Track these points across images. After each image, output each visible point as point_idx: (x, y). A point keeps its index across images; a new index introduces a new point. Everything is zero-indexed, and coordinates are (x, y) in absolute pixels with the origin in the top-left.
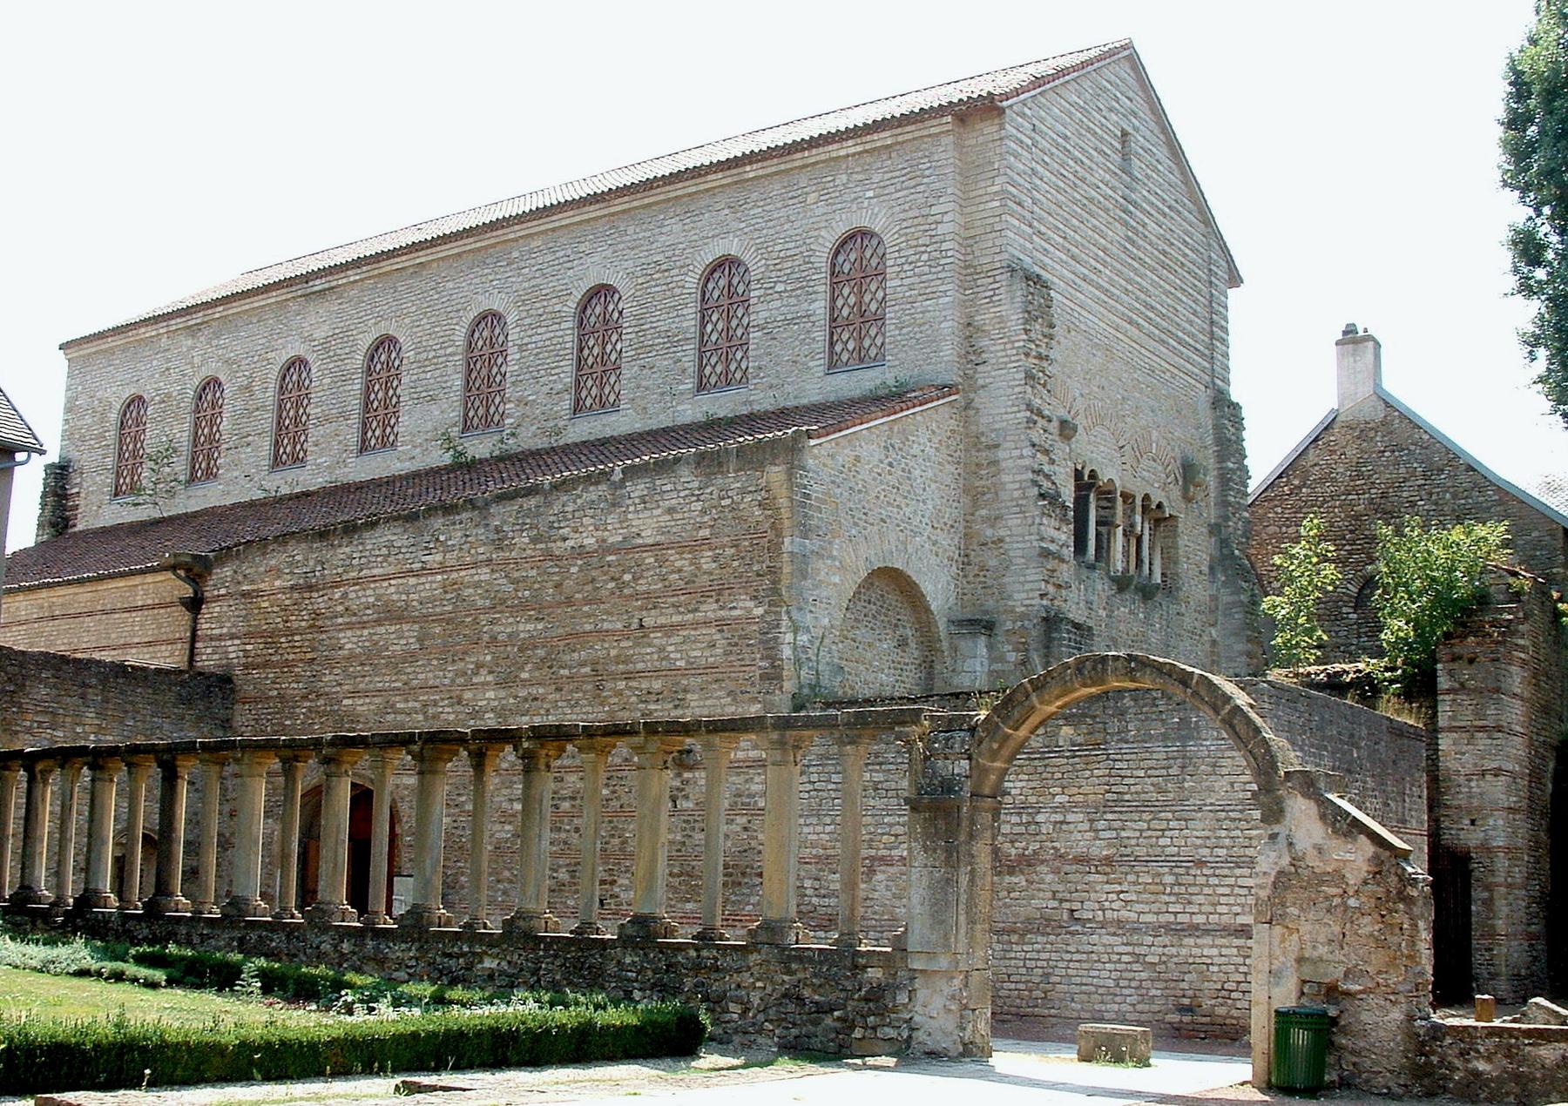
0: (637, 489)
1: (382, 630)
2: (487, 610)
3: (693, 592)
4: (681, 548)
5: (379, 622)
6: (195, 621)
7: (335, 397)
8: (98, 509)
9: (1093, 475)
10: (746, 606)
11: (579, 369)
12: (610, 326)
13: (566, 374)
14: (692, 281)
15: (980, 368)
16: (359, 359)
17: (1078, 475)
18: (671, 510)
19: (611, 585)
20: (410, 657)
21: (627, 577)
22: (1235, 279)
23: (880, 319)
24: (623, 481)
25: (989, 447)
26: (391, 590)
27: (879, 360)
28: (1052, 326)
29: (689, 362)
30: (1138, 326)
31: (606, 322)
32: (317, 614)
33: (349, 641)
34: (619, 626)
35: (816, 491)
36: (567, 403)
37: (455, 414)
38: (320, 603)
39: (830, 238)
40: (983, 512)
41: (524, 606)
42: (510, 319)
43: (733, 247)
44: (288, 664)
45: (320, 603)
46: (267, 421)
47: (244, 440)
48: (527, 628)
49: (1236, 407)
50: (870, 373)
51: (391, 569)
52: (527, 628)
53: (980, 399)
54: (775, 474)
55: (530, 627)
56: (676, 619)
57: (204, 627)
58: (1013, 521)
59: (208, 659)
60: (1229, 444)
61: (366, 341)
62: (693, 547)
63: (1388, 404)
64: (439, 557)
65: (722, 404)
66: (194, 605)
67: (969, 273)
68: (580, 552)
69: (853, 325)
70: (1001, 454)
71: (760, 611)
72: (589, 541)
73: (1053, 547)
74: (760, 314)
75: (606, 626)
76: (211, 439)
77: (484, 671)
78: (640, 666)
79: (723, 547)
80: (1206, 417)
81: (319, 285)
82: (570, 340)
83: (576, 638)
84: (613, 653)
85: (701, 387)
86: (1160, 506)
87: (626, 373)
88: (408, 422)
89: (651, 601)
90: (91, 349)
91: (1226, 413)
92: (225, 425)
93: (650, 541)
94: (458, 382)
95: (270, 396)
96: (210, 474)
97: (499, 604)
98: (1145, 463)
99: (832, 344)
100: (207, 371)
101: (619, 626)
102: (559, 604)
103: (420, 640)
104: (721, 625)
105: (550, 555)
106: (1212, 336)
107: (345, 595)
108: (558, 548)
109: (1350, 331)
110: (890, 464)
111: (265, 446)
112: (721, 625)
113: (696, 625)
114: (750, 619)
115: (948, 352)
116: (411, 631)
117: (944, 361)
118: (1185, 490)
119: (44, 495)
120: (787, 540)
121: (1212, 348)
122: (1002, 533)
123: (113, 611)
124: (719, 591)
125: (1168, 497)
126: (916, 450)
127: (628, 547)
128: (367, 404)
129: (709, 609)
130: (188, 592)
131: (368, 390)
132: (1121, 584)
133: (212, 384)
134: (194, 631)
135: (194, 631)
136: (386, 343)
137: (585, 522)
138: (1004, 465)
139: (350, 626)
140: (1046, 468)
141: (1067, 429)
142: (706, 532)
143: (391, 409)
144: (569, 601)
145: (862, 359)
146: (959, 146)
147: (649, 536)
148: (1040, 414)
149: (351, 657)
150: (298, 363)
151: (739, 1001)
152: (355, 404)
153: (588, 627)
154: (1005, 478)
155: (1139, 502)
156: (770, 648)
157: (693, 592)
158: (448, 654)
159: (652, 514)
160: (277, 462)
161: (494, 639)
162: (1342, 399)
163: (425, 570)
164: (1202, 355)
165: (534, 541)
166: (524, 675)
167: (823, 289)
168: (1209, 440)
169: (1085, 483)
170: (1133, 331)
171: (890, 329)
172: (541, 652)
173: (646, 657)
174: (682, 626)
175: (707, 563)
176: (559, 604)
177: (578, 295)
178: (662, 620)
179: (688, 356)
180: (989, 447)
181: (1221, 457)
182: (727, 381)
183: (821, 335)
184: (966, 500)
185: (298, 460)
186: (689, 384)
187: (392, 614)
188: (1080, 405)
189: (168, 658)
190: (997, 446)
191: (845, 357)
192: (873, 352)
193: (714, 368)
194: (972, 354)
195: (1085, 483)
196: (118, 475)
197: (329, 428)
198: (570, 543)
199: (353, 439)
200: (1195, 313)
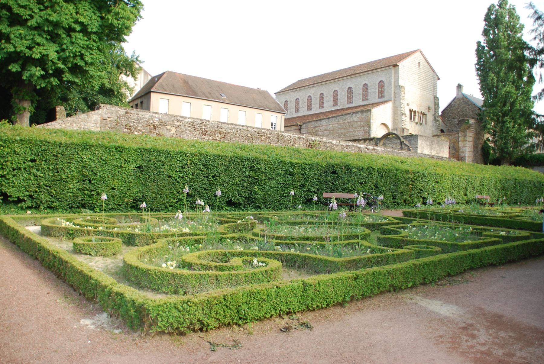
0: (354, 115)
3: (361, 127)
7: (316, 101)
10: (366, 128)
13: (346, 98)
16: (318, 96)
22: (439, 79)
26: (326, 127)
38: (317, 129)
43: (366, 82)
47: (303, 107)
48: (342, 131)
52: (342, 131)
60: (436, 105)
61: (319, 94)
63: (463, 95)
65: (366, 103)
68: (348, 122)
74: (370, 91)
83: (348, 132)
88: (325, 105)
89: (356, 128)
91: (436, 98)
94: (332, 99)
97: (339, 128)
109: (459, 84)
116: (328, 132)
124: (363, 127)
125: (426, 112)
127: (353, 122)
129: (362, 129)
132: (417, 123)
133: (297, 99)
136: (322, 94)
137: (348, 119)
141: (408, 105)
145: (382, 97)
150: (310, 96)
157: (361, 127)
162: (457, 94)
167: (377, 88)
173: (355, 134)
175: (362, 123)
182: (366, 100)
185: (311, 110)
187: (326, 130)
195: (411, 111)
199: (318, 107)
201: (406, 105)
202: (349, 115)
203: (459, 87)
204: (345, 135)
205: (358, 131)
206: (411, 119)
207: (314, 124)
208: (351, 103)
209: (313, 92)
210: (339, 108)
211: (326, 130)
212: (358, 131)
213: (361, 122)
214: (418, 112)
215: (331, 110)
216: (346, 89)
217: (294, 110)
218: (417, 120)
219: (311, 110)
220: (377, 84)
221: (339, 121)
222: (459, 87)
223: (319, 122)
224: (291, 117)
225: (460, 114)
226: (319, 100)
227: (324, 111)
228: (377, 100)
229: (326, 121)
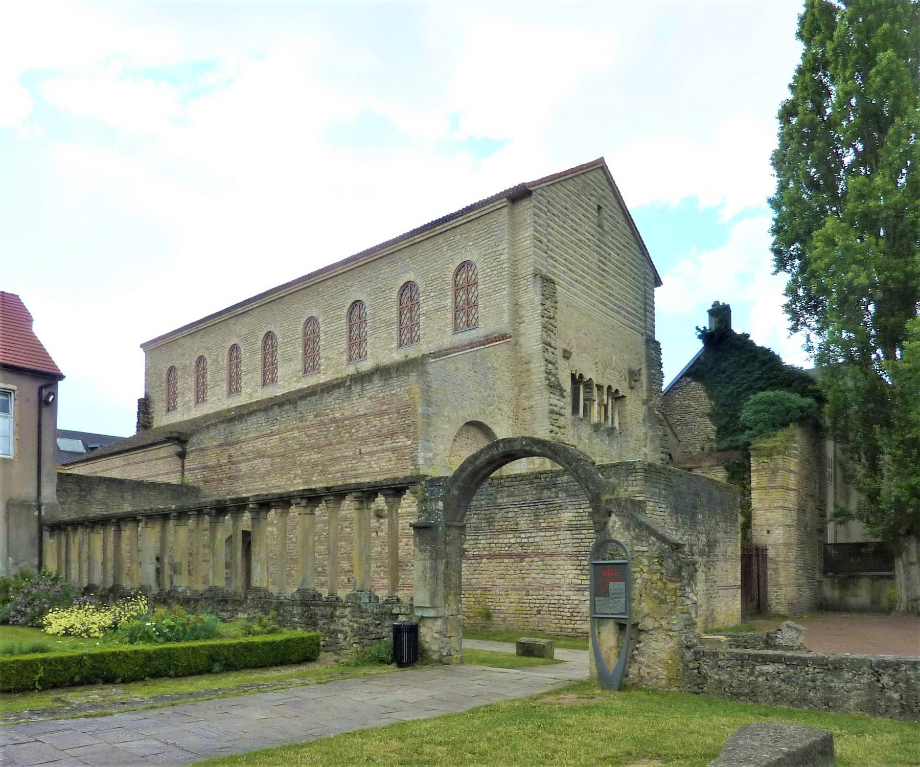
0: (356, 389)
1: (256, 462)
2: (297, 450)
3: (381, 436)
4: (375, 415)
5: (255, 458)
6: (183, 462)
8: (162, 420)
9: (581, 375)
11: (350, 340)
12: (362, 320)
13: (344, 344)
14: (395, 295)
15: (522, 325)
17: (573, 376)
18: (370, 398)
19: (347, 435)
20: (268, 473)
21: (354, 431)
23: (476, 305)
24: (350, 386)
25: (526, 363)
27: (476, 326)
28: (556, 302)
29: (395, 335)
30: (605, 305)
31: (360, 318)
32: (230, 456)
33: (244, 467)
34: (351, 453)
35: (435, 385)
36: (345, 357)
37: (300, 366)
40: (524, 394)
41: (312, 448)
42: (320, 320)
44: (221, 480)
46: (224, 374)
47: (216, 384)
48: (315, 457)
49: (658, 344)
50: (472, 332)
51: (258, 434)
52: (315, 457)
53: (522, 340)
54: (413, 377)
55: (315, 456)
56: (375, 449)
57: (188, 464)
58: (538, 397)
59: (189, 479)
64: (277, 427)
66: (182, 455)
68: (335, 420)
70: (532, 366)
71: (409, 443)
72: (338, 415)
73: (556, 409)
75: (346, 454)
76: (203, 384)
77: (298, 478)
78: (360, 471)
79: (392, 413)
80: (642, 349)
81: (240, 310)
83: (335, 460)
84: (349, 466)
86: (617, 391)
88: (281, 372)
89: (364, 441)
91: (653, 348)
92: (208, 376)
93: (362, 413)
95: (225, 363)
96: (204, 400)
97: (303, 447)
98: (608, 370)
99: (456, 319)
100: (199, 354)
101: (351, 453)
102: (327, 445)
103: (272, 465)
104: (394, 450)
105: (322, 423)
106: (646, 310)
107: (241, 447)
108: (325, 419)
110: (475, 372)
111: (225, 386)
112: (394, 450)
113: (383, 451)
114: (406, 447)
115: (506, 318)
116: (267, 461)
117: (503, 324)
118: (630, 382)
119: (138, 413)
120: (420, 409)
121: (645, 316)
122: (533, 403)
123: (152, 460)
124: (392, 434)
126: (489, 365)
129: (388, 443)
130: (180, 449)
131: (265, 358)
132: (596, 427)
134: (183, 467)
135: (183, 467)
138: (533, 370)
139: (244, 461)
140: (553, 372)
141: (567, 355)
142: (385, 407)
144: (331, 444)
145: (469, 326)
147: (362, 411)
148: (550, 345)
149: (245, 474)
151: (341, 632)
153: (339, 455)
154: (534, 377)
155: (605, 389)
156: (414, 459)
158: (283, 470)
161: (301, 463)
163: (272, 434)
164: (640, 319)
165: (316, 416)
166: (314, 479)
168: (643, 360)
169: (577, 380)
170: (602, 307)
171: (481, 310)
172: (321, 468)
174: (377, 452)
176: (327, 445)
177: (348, 306)
178: (369, 450)
180: (526, 363)
181: (649, 367)
183: (450, 316)
184: (517, 389)
185: (238, 391)
186: (395, 344)
188: (574, 342)
189: (174, 480)
190: (529, 362)
191: (461, 325)
192: (474, 321)
195: (577, 380)
196: (169, 403)
197: (249, 376)
198: (330, 416)
199: (259, 378)
200: (636, 299)
201: (559, 352)
202: (336, 393)
203: (697, 328)
205: (371, 454)
206: (575, 410)
210: (322, 378)
211: (261, 455)
212: (371, 454)
213: (382, 413)
214: (600, 387)
216: (345, 311)
218: (595, 417)
219: (238, 391)
221: (302, 419)
223: (239, 427)
224: (186, 418)
226: (259, 356)
227: (279, 393)
228: (448, 339)
229: (261, 418)
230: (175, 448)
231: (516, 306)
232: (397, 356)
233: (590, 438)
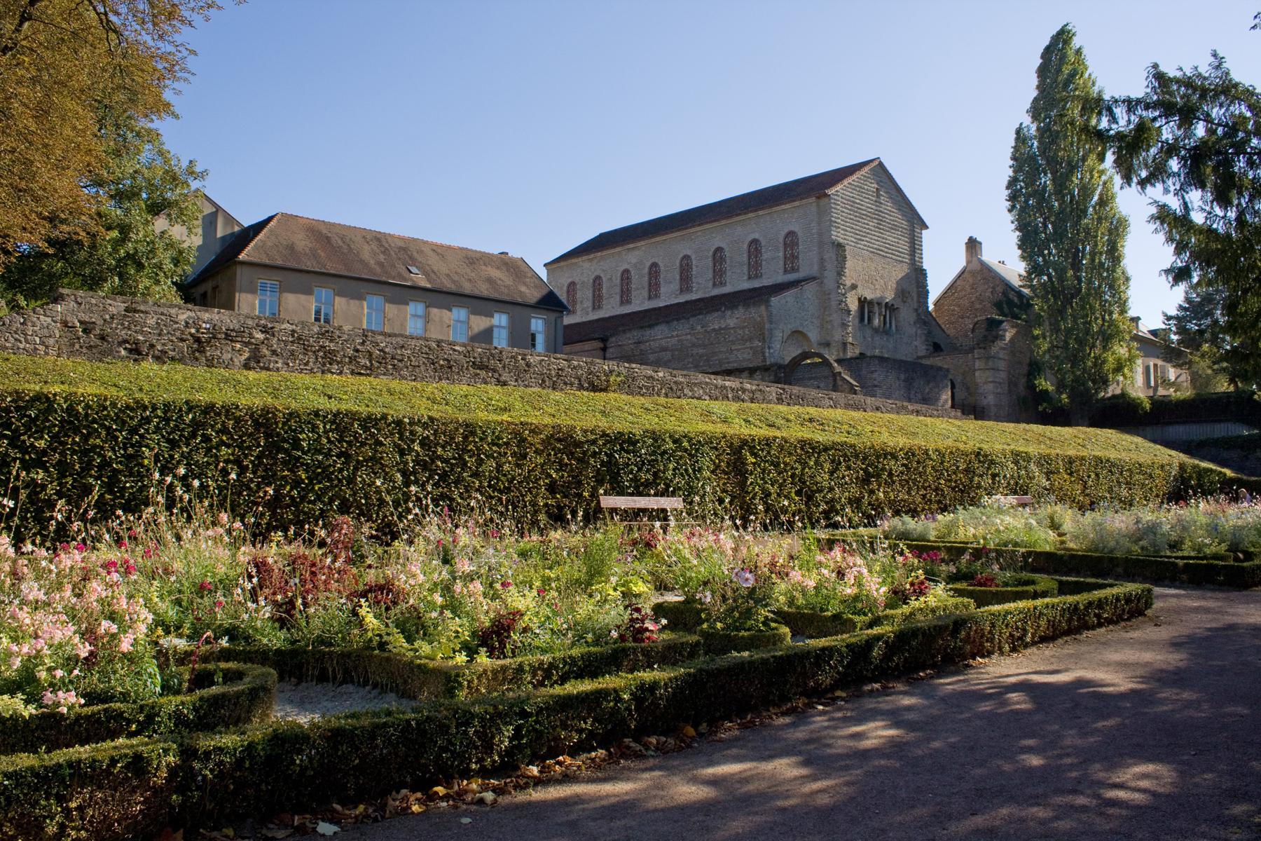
10: (757, 343)
13: (710, 274)
14: (745, 246)
16: (646, 270)
23: (797, 257)
26: (663, 342)
29: (745, 271)
35: (775, 312)
36: (711, 283)
37: (678, 287)
38: (643, 347)
39: (783, 233)
43: (756, 236)
45: (643, 347)
46: (618, 290)
54: (763, 308)
61: (648, 264)
62: (743, 328)
63: (982, 263)
65: (756, 284)
67: (821, 244)
68: (714, 330)
69: (791, 260)
74: (765, 256)
82: (711, 264)
85: (749, 278)
87: (728, 274)
88: (663, 290)
89: (733, 342)
90: (555, 266)
92: (604, 291)
94: (678, 277)
95: (618, 281)
96: (599, 307)
97: (694, 345)
109: (971, 238)
111: (618, 298)
115: (816, 267)
117: (814, 271)
124: (750, 339)
127: (726, 328)
128: (650, 285)
129: (748, 344)
130: (602, 345)
131: (650, 279)
133: (598, 278)
136: (654, 265)
137: (715, 322)
143: (658, 285)
145: (794, 270)
146: (818, 206)
147: (732, 325)
150: (626, 271)
152: (646, 285)
156: (763, 353)
159: (733, 319)
160: (622, 303)
162: (968, 262)
167: (782, 249)
179: (745, 268)
181: (918, 287)
182: (756, 277)
183: (782, 263)
187: (664, 349)
193: (753, 273)
194: (822, 267)
199: (646, 294)
204: (708, 360)
205: (738, 350)
206: (862, 319)
207: (636, 334)
208: (722, 284)
209: (634, 261)
210: (694, 297)
212: (738, 350)
213: (743, 328)
215: (676, 301)
217: (588, 304)
218: (876, 322)
220: (781, 240)
221: (692, 329)
222: (973, 245)
225: (978, 306)
226: (646, 279)
228: (781, 278)
230: (602, 345)
231: (822, 261)
232: (746, 285)
233: (872, 337)
